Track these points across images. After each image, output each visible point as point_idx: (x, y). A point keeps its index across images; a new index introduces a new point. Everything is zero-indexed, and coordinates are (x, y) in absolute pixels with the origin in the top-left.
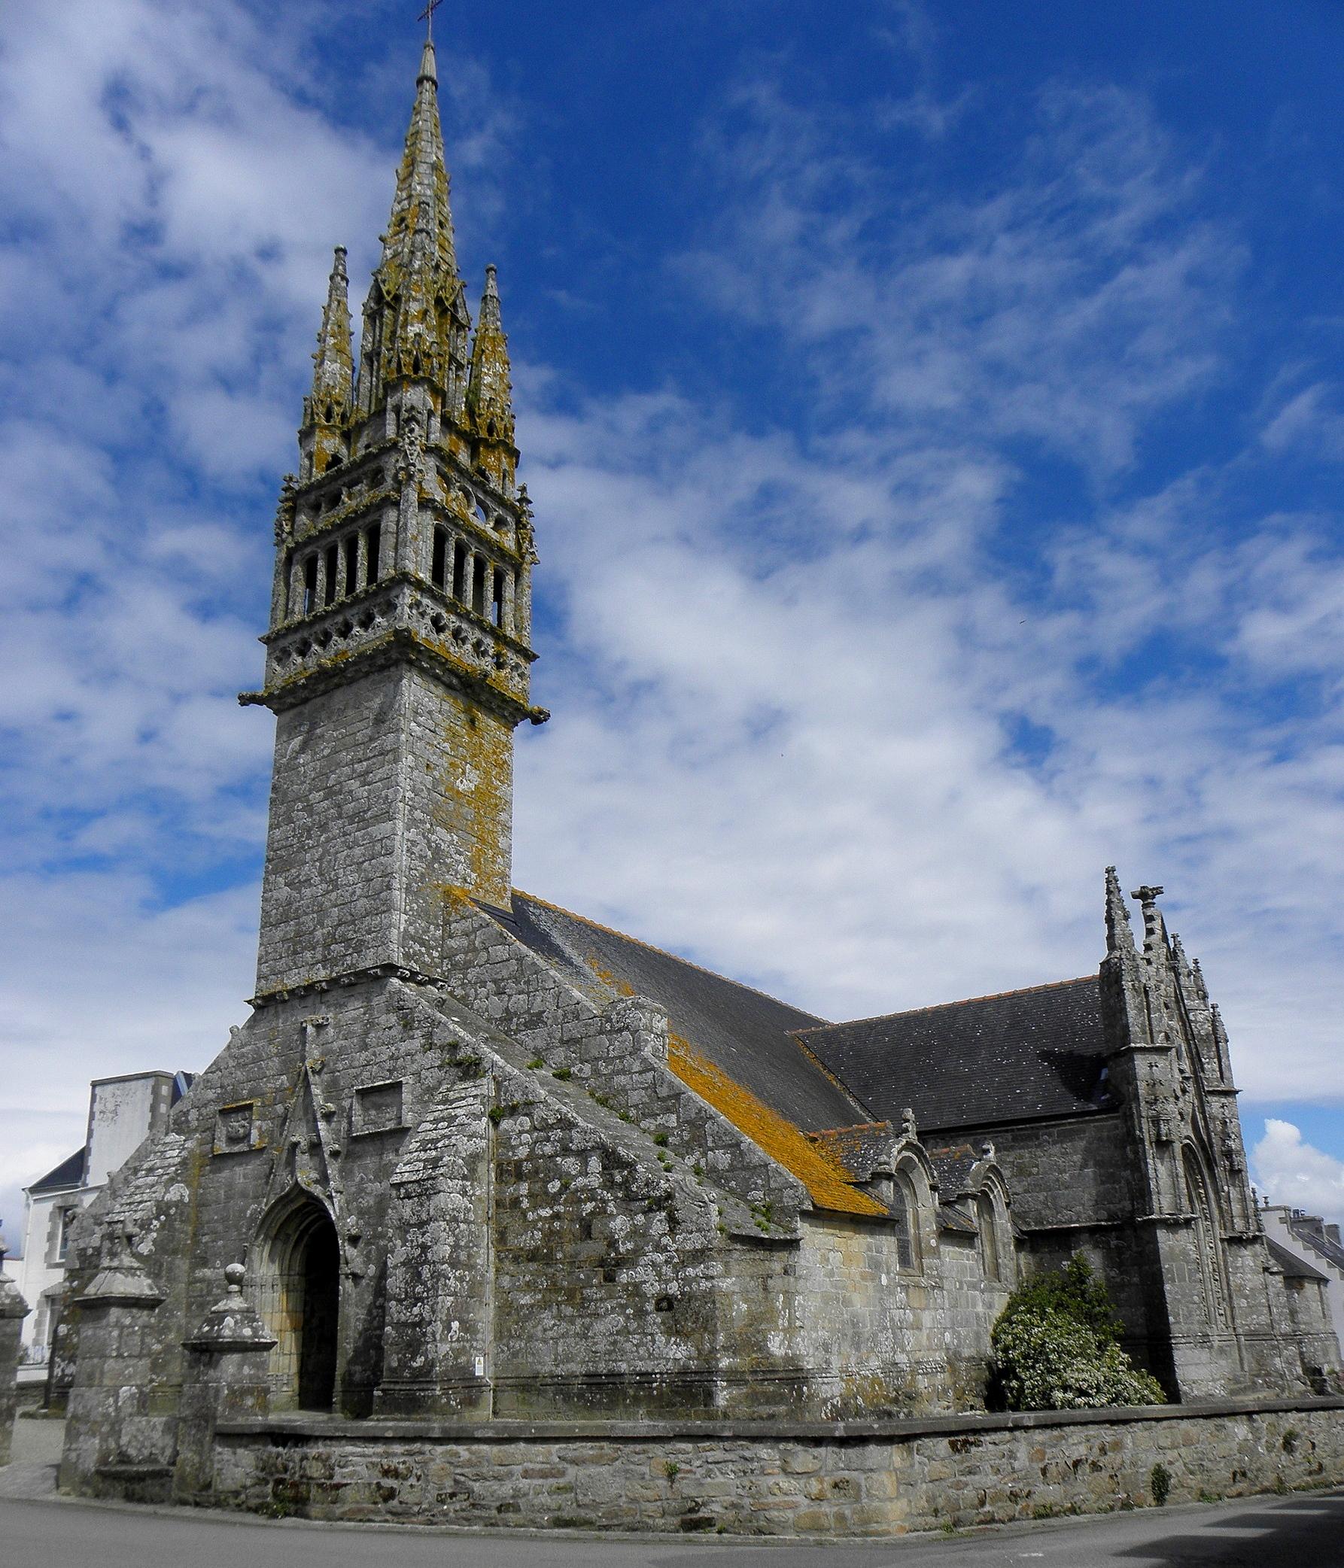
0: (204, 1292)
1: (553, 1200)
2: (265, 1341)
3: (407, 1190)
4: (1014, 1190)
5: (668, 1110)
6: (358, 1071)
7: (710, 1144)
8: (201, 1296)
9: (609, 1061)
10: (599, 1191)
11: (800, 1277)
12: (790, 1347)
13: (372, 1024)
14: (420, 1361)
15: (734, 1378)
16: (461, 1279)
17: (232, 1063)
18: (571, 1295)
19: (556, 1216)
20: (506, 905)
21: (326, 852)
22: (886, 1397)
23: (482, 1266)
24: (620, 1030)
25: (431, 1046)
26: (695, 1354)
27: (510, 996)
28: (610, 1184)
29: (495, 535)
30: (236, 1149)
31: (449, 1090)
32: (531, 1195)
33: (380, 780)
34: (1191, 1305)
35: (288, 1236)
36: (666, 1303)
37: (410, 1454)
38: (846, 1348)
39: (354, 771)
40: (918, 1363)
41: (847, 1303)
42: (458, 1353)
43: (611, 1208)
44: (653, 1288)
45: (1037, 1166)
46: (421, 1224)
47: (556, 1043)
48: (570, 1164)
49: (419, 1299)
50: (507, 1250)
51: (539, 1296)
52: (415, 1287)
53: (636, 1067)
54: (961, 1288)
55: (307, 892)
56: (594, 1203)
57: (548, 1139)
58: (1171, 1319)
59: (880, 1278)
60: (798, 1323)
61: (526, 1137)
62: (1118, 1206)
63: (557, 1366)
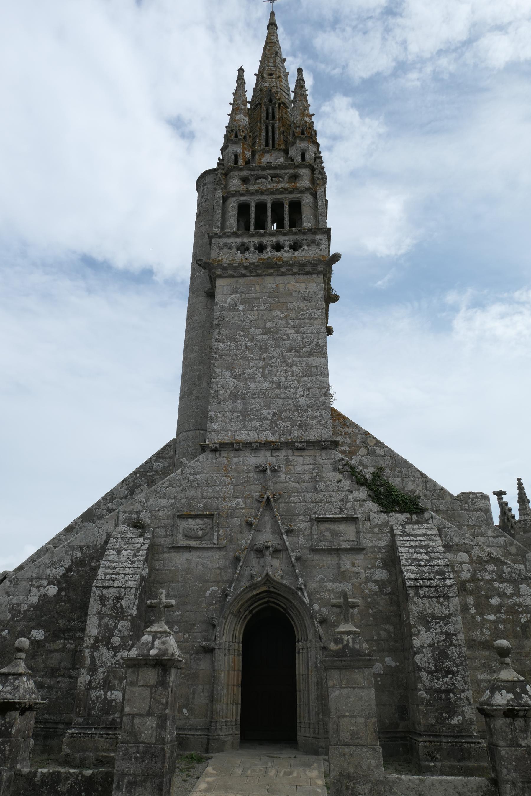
13: (321, 477)
24: (475, 510)
30: (193, 543)
33: (312, 333)
39: (288, 323)
57: (485, 570)
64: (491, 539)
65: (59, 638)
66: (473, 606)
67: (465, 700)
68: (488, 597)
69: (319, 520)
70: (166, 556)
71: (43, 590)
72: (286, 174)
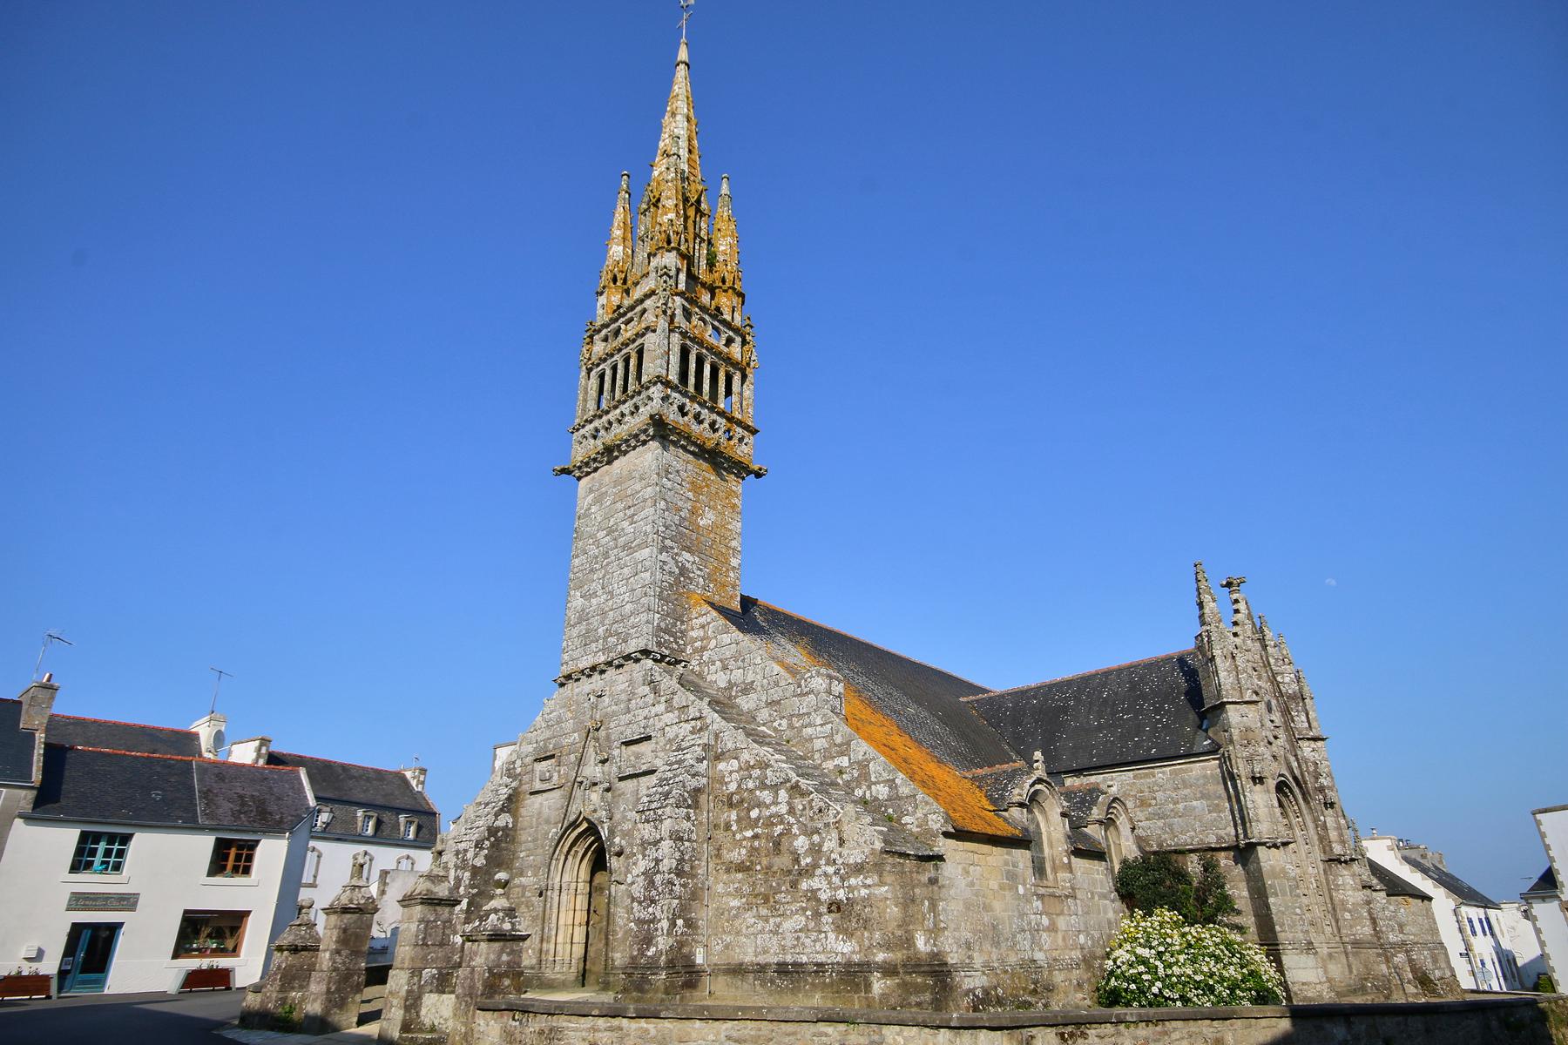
0: (520, 895)
1: (754, 824)
2: (520, 933)
4: (1137, 818)
5: (842, 754)
7: (873, 779)
8: (518, 898)
9: (800, 716)
10: (786, 816)
11: (943, 886)
12: (935, 945)
13: (634, 694)
15: (889, 970)
16: (684, 886)
18: (766, 900)
19: (756, 837)
20: (736, 605)
21: (607, 572)
22: (1024, 989)
23: (703, 875)
24: (807, 694)
25: (669, 709)
26: (857, 949)
27: (731, 670)
29: (726, 350)
31: (682, 740)
32: (739, 821)
34: (1294, 917)
35: (577, 852)
36: (835, 906)
37: (611, 1029)
38: (987, 946)
40: (1055, 960)
41: (987, 908)
42: (681, 944)
43: (795, 830)
44: (824, 896)
45: (1155, 799)
46: (656, 843)
47: (763, 705)
48: (766, 796)
49: (653, 901)
50: (722, 863)
51: (744, 900)
52: (650, 891)
53: (819, 721)
54: (1093, 897)
55: (594, 601)
56: (782, 826)
58: (1278, 928)
59: (1017, 888)
60: (942, 925)
61: (735, 775)
62: (1225, 831)
63: (756, 956)
64: (819, 728)
66: (736, 821)
67: (660, 930)
68: (749, 810)
69: (628, 744)
70: (528, 802)
72: (635, 314)
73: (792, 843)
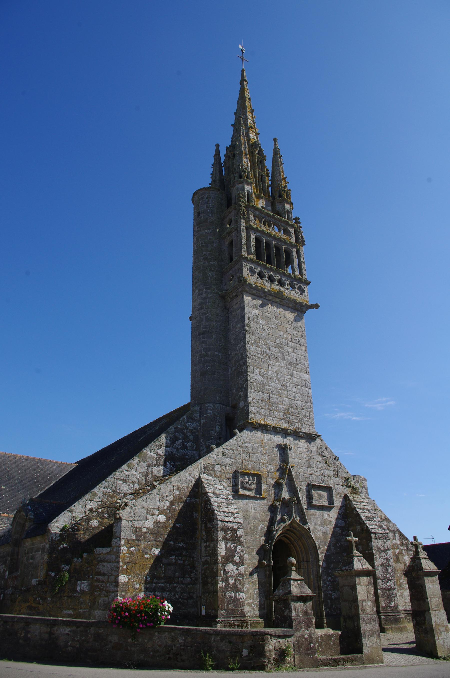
3: (378, 536)
6: (308, 476)
14: (393, 604)
17: (239, 449)
28: (402, 544)
46: (385, 551)
49: (389, 580)
52: (387, 575)
65: (172, 555)
71: (155, 517)
73: (403, 558)
